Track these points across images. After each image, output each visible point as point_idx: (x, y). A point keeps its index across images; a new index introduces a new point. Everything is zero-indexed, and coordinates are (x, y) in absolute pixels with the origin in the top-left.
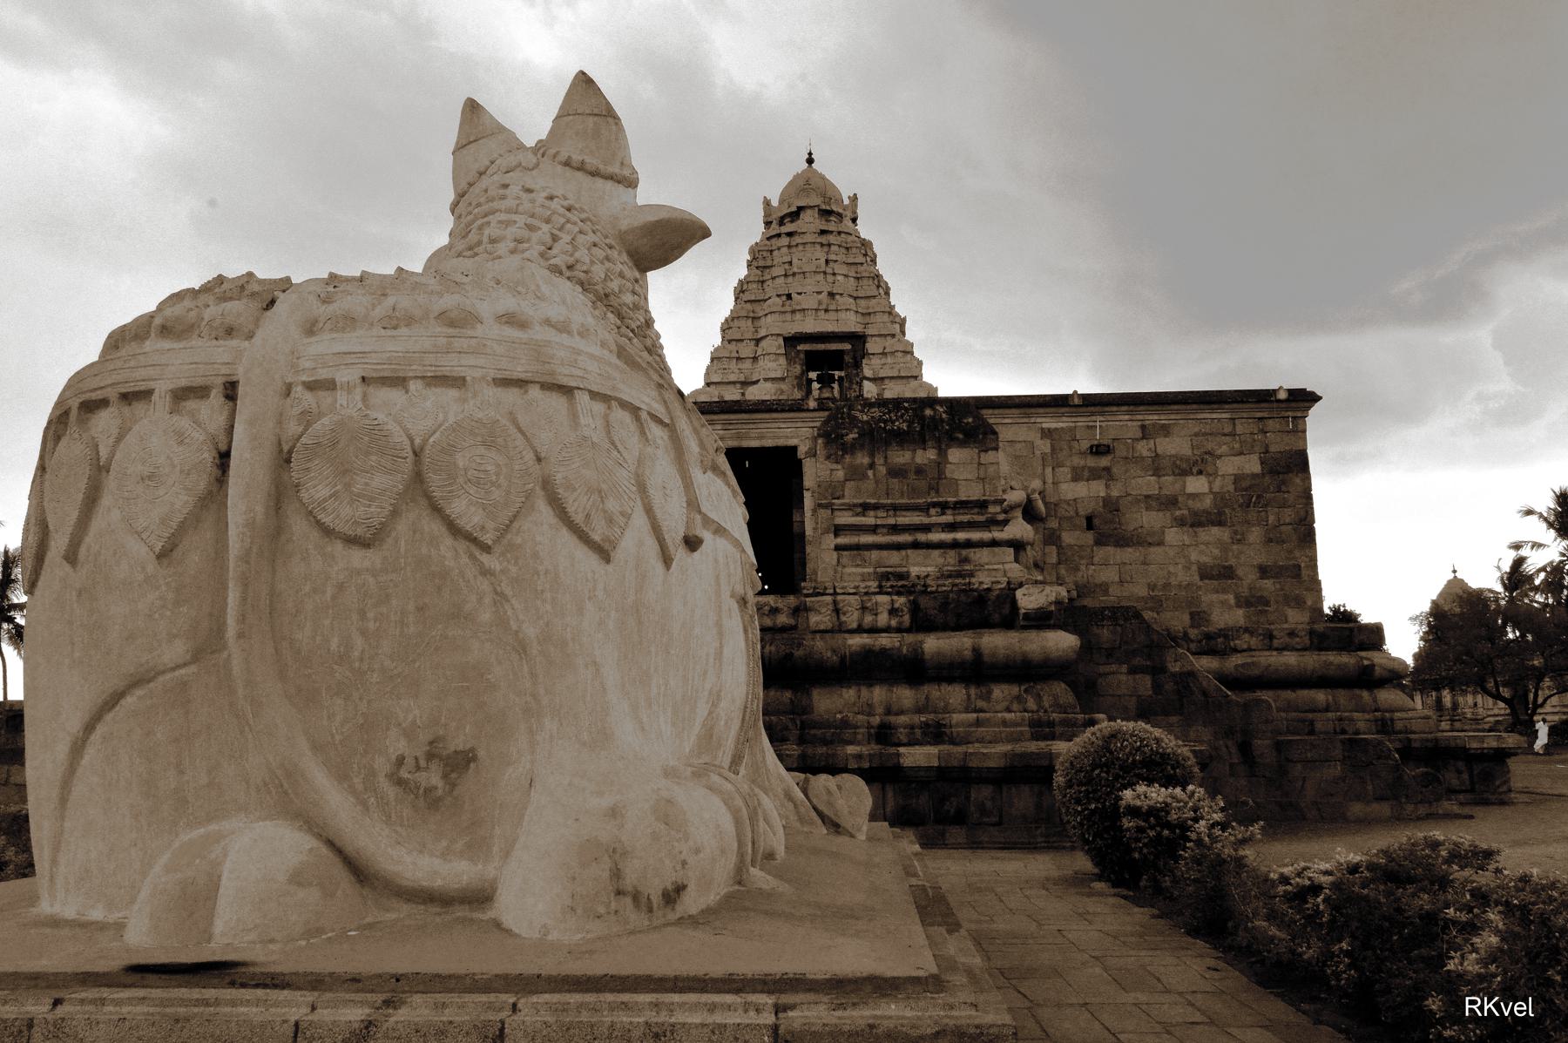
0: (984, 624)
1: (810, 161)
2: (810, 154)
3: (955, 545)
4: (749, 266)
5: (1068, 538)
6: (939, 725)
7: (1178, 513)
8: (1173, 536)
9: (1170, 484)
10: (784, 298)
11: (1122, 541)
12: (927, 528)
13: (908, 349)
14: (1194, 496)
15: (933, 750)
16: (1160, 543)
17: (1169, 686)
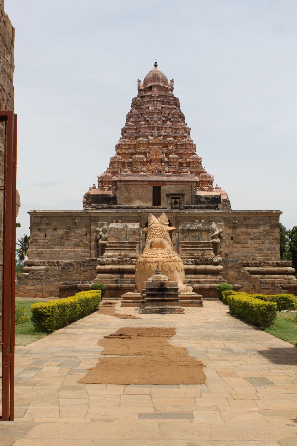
0: (208, 264)
1: (156, 66)
2: (156, 63)
3: (203, 250)
4: (132, 107)
5: (228, 241)
6: (199, 281)
7: (251, 237)
8: (250, 242)
9: (249, 230)
10: (146, 122)
11: (238, 243)
12: (198, 247)
13: (192, 143)
14: (254, 233)
15: (198, 285)
16: (247, 243)
17: (241, 274)
